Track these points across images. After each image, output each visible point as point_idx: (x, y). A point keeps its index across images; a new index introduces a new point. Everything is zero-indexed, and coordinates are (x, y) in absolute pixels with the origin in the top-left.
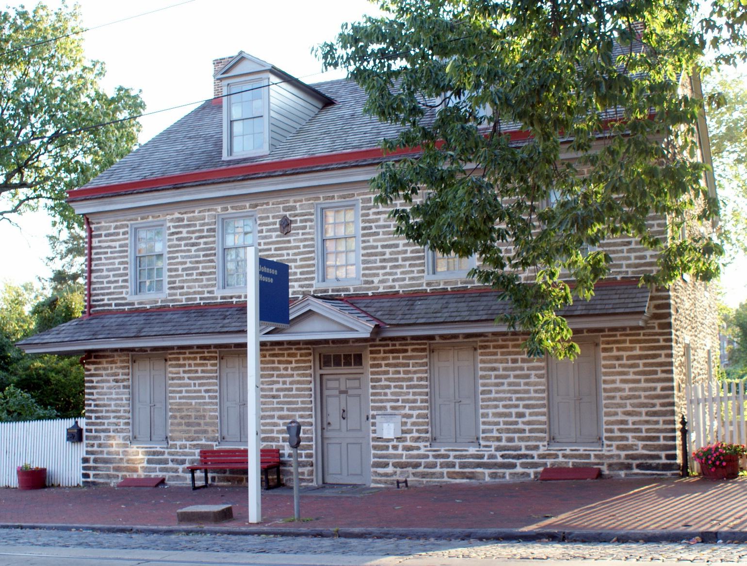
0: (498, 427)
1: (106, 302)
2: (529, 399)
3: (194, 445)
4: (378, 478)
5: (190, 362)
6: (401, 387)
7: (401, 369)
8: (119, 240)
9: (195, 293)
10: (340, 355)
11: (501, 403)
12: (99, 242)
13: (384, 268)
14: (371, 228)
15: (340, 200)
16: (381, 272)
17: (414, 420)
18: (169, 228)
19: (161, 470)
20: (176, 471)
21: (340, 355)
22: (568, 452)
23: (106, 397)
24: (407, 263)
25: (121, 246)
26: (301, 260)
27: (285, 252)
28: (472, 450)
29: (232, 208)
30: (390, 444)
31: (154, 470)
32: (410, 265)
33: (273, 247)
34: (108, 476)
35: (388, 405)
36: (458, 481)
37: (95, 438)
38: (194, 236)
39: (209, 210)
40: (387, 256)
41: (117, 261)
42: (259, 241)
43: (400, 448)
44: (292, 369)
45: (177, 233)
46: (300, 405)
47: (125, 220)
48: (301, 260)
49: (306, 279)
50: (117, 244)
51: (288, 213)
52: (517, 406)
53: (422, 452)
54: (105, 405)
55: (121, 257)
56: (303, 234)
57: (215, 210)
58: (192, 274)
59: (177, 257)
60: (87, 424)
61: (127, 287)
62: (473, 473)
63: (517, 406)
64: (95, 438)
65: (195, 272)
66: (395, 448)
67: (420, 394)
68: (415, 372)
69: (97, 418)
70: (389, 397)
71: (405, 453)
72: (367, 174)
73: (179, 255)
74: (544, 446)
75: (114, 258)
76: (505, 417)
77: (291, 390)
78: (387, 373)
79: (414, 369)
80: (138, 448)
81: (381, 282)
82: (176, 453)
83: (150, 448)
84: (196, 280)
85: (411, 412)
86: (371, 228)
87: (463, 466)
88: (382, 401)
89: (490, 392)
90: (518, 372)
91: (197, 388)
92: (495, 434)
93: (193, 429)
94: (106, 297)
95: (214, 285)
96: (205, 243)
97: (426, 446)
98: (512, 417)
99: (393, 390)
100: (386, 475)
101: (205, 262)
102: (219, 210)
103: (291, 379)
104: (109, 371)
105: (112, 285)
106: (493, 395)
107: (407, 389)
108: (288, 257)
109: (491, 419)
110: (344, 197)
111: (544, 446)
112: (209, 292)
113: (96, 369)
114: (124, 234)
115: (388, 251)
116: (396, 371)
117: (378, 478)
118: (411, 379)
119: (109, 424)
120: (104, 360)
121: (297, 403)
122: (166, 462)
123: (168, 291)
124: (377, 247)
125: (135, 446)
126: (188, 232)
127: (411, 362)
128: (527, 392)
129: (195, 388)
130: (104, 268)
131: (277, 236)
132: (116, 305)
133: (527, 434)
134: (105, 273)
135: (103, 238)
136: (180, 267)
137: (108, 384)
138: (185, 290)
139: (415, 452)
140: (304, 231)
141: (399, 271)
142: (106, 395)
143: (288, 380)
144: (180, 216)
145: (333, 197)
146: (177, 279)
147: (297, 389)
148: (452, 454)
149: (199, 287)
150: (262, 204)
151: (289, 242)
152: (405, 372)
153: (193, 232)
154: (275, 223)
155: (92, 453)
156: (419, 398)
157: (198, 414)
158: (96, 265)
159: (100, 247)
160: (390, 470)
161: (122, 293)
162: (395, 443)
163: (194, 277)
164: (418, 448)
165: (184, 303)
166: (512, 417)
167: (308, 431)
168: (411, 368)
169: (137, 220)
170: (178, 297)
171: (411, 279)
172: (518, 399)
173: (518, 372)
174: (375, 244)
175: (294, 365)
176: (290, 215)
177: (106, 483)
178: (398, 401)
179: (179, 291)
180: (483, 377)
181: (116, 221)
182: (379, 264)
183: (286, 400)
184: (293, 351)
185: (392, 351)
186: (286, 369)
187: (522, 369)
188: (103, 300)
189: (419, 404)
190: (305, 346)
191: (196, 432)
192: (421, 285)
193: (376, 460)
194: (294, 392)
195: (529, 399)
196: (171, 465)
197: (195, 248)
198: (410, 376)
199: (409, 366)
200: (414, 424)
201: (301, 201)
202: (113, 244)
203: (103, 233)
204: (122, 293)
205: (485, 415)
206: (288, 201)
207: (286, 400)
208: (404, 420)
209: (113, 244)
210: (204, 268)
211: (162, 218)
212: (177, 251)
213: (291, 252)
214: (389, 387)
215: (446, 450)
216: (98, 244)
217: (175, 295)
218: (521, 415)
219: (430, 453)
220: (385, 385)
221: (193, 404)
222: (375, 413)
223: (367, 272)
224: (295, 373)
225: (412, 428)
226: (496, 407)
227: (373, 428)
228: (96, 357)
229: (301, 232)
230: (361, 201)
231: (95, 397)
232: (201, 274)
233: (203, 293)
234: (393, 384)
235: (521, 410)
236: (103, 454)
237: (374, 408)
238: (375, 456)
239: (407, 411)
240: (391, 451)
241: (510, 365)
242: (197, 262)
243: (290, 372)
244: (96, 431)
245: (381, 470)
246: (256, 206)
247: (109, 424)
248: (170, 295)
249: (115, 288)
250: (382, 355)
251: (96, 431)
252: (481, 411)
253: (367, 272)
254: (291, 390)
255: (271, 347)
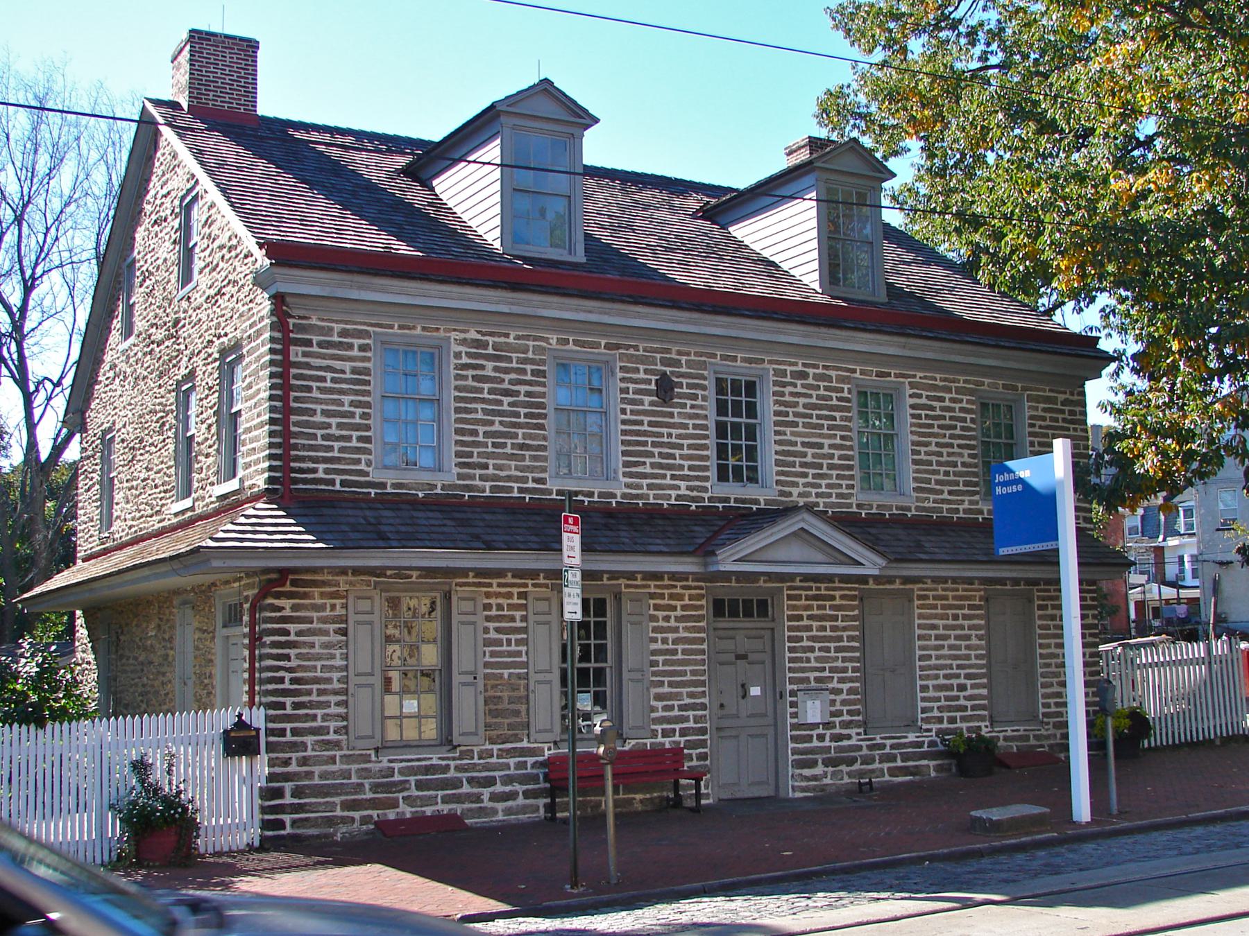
0: (939, 704)
1: (321, 475)
2: (970, 666)
3: (508, 751)
4: (804, 784)
5: (500, 601)
6: (828, 650)
7: (828, 624)
8: (350, 359)
9: (509, 478)
10: (752, 600)
11: (942, 673)
12: (305, 354)
13: (805, 475)
14: (787, 415)
15: (743, 364)
16: (801, 481)
17: (844, 696)
18: (458, 355)
19: (446, 800)
20: (478, 798)
21: (724, 600)
22: (1009, 733)
23: (319, 664)
24: (834, 473)
25: (354, 371)
26: (690, 447)
27: (665, 430)
28: (912, 737)
29: (576, 342)
30: (815, 733)
31: (432, 801)
32: (838, 476)
33: (646, 419)
34: (330, 821)
35: (812, 675)
36: (900, 779)
37: (293, 746)
38: (507, 377)
39: (536, 339)
40: (809, 459)
41: (347, 399)
42: (624, 406)
43: (827, 738)
44: (677, 619)
45: (475, 367)
46: (688, 677)
47: (365, 324)
48: (690, 447)
49: (697, 478)
50: (347, 366)
51: (668, 370)
52: (958, 676)
53: (853, 742)
54: (316, 681)
55: (357, 393)
56: (692, 407)
57: (546, 340)
58: (504, 445)
59: (476, 411)
60: (269, 719)
61: (367, 451)
62: (916, 766)
63: (958, 676)
64: (293, 746)
65: (509, 441)
66: (821, 738)
67: (851, 660)
68: (845, 629)
69: (296, 706)
70: (813, 664)
71: (833, 744)
72: (804, 336)
73: (479, 406)
74: (986, 727)
75: (342, 392)
76: (946, 691)
77: (675, 652)
78: (809, 628)
79: (844, 624)
80: (390, 761)
81: (800, 495)
82: (473, 767)
83: (419, 760)
84: (512, 457)
85: (841, 686)
86: (787, 415)
87: (906, 757)
88: (803, 670)
89: (929, 657)
90: (959, 632)
91: (513, 648)
92: (936, 713)
93: (507, 721)
94: (321, 467)
95: (544, 470)
96: (528, 394)
97: (858, 734)
98: (953, 690)
99: (817, 654)
100: (815, 778)
101: (527, 426)
102: (554, 342)
103: (675, 635)
104: (328, 613)
105: (336, 445)
106: (933, 662)
107: (677, 650)
108: (669, 440)
109: (931, 694)
110: (749, 361)
111: (986, 727)
112: (535, 480)
113: (295, 608)
114: (363, 348)
115: (810, 451)
116: (821, 626)
117: (804, 784)
118: (840, 639)
119: (326, 717)
120: (316, 591)
121: (684, 673)
122: (456, 783)
123: (455, 470)
124: (795, 444)
125: (385, 759)
126: (496, 369)
127: (840, 613)
128: (968, 657)
129: (509, 648)
130: (319, 408)
131: (652, 403)
132: (343, 483)
133: (969, 713)
134: (318, 418)
135: (315, 349)
136: (481, 429)
137: (325, 639)
138: (491, 471)
139: (845, 743)
140: (694, 402)
141: (824, 482)
142: (319, 659)
143: (671, 636)
144: (479, 337)
145: (734, 359)
146: (476, 451)
147: (684, 652)
148: (888, 742)
149: (517, 468)
150: (628, 347)
151: (671, 415)
152: (833, 629)
153: (507, 371)
154: (649, 382)
155: (287, 777)
156: (849, 665)
157: (516, 694)
158: (297, 399)
159: (308, 366)
160: (819, 770)
161: (358, 461)
162: (820, 731)
163: (508, 450)
164: (849, 737)
165: (487, 494)
166: (953, 690)
167: (701, 717)
168: (839, 623)
169: (392, 327)
170: (477, 482)
171: (839, 496)
172: (959, 667)
173: (959, 632)
174: (793, 439)
175: (679, 613)
176: (671, 372)
177: (326, 836)
178: (824, 669)
179: (478, 472)
180: (920, 637)
181: (347, 322)
182: (798, 469)
183: (667, 668)
184: (678, 590)
185: (816, 598)
186: (667, 619)
187: (962, 628)
188: (315, 471)
189: (850, 674)
190: (696, 584)
191: (511, 727)
192: (850, 505)
193: (796, 757)
194: (680, 656)
195: (970, 666)
196: (466, 789)
197: (511, 399)
198: (839, 633)
199: (837, 620)
200: (844, 702)
201: (688, 354)
202: (337, 364)
203: (315, 339)
204: (358, 461)
205: (924, 688)
206: (668, 351)
207: (667, 668)
208: (832, 697)
209: (337, 364)
210: (525, 436)
211: (442, 334)
212: (475, 400)
213: (674, 431)
214: (812, 649)
215: (881, 738)
216: (301, 359)
217: (472, 477)
218: (962, 688)
219: (864, 744)
220: (808, 647)
221: (506, 676)
222: (795, 687)
223: (783, 478)
224: (681, 625)
225: (842, 708)
226: (937, 677)
227: (794, 710)
228: (295, 583)
229: (689, 402)
230: (772, 372)
231: (294, 663)
232: (522, 447)
233: (525, 479)
234: (817, 645)
235: (962, 681)
236: (312, 778)
237: (792, 681)
238: (795, 752)
239: (834, 684)
240: (816, 743)
241: (951, 622)
242: (515, 425)
243: (673, 623)
244: (295, 732)
245: (807, 772)
246: (618, 347)
247: (326, 717)
248: (460, 476)
249: (341, 450)
250: (803, 602)
251: (295, 732)
252: (919, 683)
253: (783, 478)
254: (675, 652)
255: (644, 583)
